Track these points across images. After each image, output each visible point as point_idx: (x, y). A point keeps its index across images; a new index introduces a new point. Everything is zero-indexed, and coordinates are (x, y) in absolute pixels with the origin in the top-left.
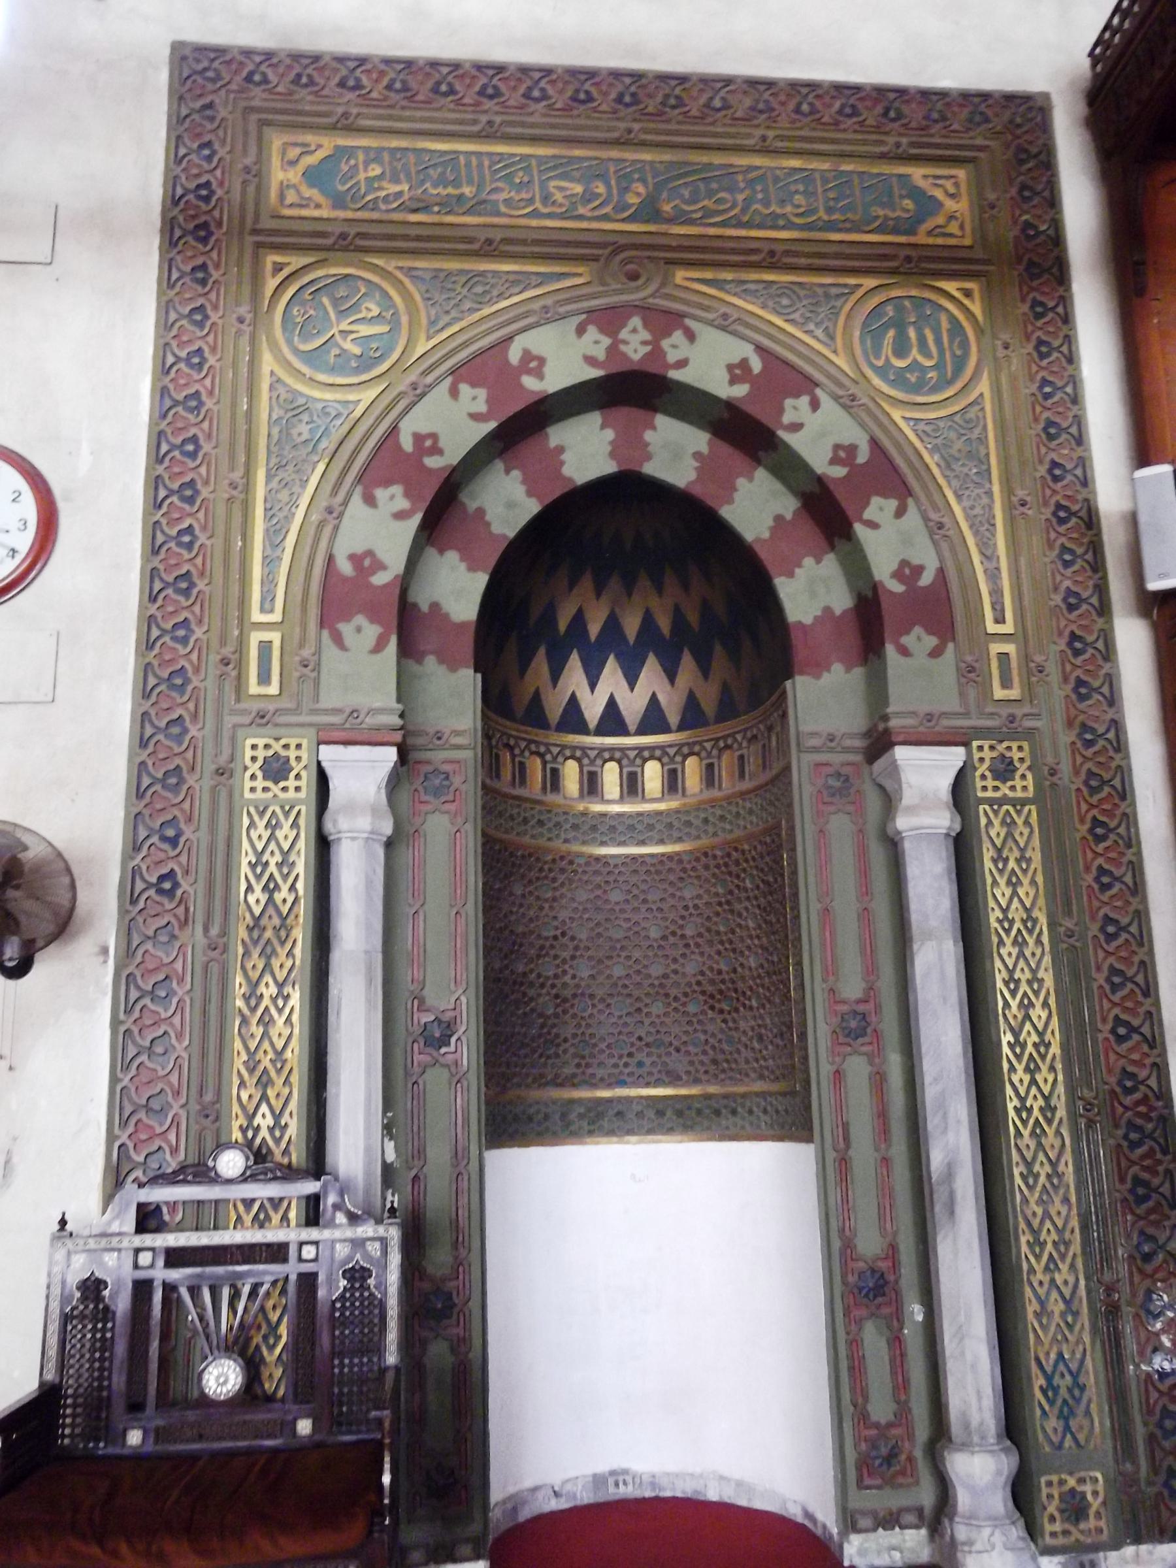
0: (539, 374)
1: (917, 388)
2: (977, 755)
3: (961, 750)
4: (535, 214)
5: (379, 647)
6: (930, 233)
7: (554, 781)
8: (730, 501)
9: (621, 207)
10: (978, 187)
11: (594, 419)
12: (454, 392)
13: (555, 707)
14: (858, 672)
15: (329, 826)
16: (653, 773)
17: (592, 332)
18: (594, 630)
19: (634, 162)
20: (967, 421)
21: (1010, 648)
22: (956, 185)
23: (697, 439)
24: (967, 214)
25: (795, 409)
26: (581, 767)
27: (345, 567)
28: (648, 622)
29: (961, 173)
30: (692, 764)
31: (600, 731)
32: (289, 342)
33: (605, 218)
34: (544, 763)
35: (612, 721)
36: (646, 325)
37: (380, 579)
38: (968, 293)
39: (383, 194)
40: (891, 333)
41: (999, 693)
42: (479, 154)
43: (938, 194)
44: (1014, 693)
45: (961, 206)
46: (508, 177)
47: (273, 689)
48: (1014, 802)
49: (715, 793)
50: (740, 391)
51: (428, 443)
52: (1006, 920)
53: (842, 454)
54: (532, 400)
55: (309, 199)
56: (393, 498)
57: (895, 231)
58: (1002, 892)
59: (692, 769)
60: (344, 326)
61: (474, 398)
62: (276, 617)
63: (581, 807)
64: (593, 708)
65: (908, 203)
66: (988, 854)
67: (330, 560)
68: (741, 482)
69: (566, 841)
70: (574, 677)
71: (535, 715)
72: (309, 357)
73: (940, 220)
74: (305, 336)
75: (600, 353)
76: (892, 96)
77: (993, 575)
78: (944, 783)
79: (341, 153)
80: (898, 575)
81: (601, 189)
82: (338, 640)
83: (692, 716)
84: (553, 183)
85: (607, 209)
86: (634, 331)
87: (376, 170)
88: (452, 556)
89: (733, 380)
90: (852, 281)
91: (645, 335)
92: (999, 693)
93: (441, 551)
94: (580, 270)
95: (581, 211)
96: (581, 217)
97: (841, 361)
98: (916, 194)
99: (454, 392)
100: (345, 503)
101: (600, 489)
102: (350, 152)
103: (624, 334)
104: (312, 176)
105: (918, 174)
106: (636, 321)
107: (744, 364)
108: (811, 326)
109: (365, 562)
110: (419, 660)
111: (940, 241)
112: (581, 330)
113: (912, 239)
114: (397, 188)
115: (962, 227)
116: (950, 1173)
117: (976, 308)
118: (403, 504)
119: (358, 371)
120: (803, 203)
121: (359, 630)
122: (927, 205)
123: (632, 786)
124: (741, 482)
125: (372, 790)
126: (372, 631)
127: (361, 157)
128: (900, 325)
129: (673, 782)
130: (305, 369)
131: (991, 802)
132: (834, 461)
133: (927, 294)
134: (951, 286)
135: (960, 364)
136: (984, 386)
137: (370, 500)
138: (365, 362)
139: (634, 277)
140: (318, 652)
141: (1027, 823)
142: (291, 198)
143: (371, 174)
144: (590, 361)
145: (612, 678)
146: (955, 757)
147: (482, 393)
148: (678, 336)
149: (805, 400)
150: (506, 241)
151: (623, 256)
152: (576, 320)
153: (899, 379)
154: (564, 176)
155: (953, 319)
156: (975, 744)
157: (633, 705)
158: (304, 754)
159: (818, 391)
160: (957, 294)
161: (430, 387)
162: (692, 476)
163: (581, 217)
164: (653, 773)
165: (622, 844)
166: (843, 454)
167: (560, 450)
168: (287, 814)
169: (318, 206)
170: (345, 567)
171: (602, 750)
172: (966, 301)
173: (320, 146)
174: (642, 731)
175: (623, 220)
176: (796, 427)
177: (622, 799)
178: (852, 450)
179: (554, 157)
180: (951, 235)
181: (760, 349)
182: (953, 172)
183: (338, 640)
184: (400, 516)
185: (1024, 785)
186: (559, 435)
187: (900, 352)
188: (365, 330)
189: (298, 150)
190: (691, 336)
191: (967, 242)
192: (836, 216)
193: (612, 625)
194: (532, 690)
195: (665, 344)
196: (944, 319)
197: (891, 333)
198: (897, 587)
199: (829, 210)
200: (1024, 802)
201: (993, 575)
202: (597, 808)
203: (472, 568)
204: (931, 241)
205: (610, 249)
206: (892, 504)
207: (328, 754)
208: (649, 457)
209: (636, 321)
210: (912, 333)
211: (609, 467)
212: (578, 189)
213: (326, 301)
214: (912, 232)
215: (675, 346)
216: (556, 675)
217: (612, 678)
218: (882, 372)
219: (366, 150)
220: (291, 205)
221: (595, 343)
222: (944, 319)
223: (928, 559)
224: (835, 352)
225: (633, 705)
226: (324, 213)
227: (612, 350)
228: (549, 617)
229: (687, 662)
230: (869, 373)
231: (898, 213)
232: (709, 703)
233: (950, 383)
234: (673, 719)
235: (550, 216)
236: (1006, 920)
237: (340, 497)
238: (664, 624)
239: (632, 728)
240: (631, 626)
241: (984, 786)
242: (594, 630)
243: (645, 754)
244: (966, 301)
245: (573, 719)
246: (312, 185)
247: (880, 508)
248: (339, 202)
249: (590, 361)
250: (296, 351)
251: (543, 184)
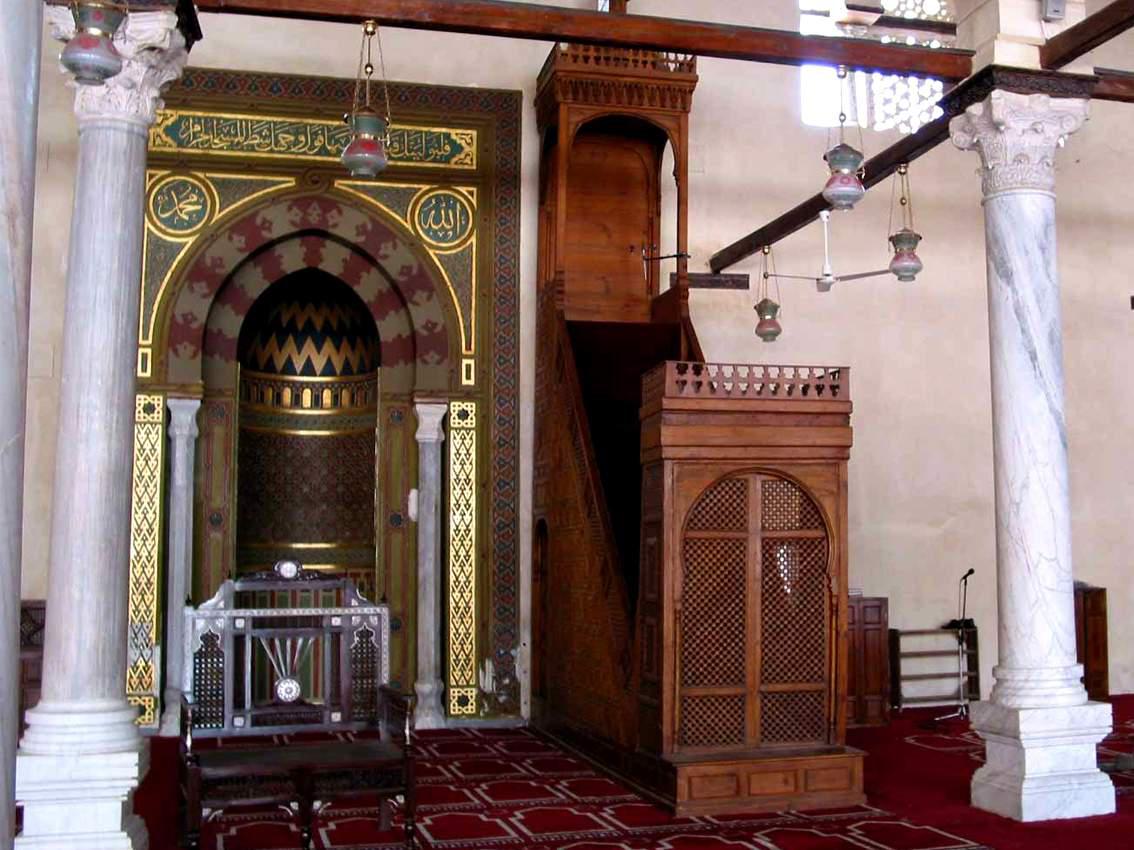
0: (269, 229)
1: (444, 239)
2: (452, 409)
3: (446, 406)
4: (272, 151)
5: (195, 355)
6: (456, 163)
7: (278, 398)
8: (358, 283)
9: (312, 147)
10: (481, 140)
11: (297, 241)
12: (230, 238)
13: (280, 363)
14: (410, 366)
15: (171, 433)
16: (327, 396)
17: (295, 210)
18: (300, 326)
19: (319, 125)
20: (464, 257)
21: (471, 362)
22: (471, 138)
23: (345, 253)
24: (475, 152)
25: (386, 249)
26: (292, 391)
27: (180, 320)
28: (327, 322)
29: (474, 133)
30: (345, 393)
31: (303, 374)
32: (156, 214)
33: (304, 153)
34: (274, 390)
35: (309, 370)
36: (321, 207)
37: (195, 325)
38: (471, 193)
39: (200, 140)
40: (433, 212)
41: (465, 382)
42: (246, 121)
43: (463, 143)
44: (471, 382)
45: (474, 149)
46: (260, 133)
47: (148, 374)
48: (466, 429)
49: (354, 409)
50: (361, 239)
51: (218, 262)
52: (458, 480)
53: (405, 270)
54: (265, 242)
55: (166, 142)
56: (201, 287)
57: (440, 162)
58: (458, 467)
59: (345, 395)
60: (181, 206)
61: (240, 241)
62: (150, 342)
63: (291, 411)
64: (299, 364)
65: (448, 148)
66: (453, 451)
67: (173, 316)
68: (364, 274)
69: (283, 428)
70: (290, 346)
71: (270, 367)
72: (163, 221)
73: (462, 156)
74: (162, 212)
75: (297, 219)
76: (445, 92)
77: (468, 329)
78: (439, 419)
79: (181, 118)
80: (425, 327)
81: (302, 138)
82: (175, 351)
83: (347, 369)
84: (280, 135)
85: (305, 149)
86: (315, 209)
87: (198, 128)
88: (228, 307)
89: (358, 234)
90: (416, 186)
91: (319, 212)
92: (465, 382)
93: (224, 304)
94: (287, 179)
95: (293, 150)
96: (293, 153)
97: (408, 226)
98: (453, 143)
99: (230, 238)
100: (180, 289)
101: (298, 274)
102: (187, 118)
103: (310, 211)
104: (169, 131)
105: (454, 133)
106: (315, 204)
107: (364, 226)
108: (396, 208)
109: (189, 318)
110: (212, 356)
111: (460, 167)
112: (290, 208)
113: (448, 166)
114: (207, 137)
115: (472, 160)
116: (425, 579)
117: (474, 202)
118: (206, 291)
119: (190, 226)
120: (398, 146)
121: (185, 348)
122: (457, 148)
123: (317, 402)
124: (364, 274)
125: (190, 418)
126: (191, 349)
127: (191, 121)
128: (437, 208)
129: (336, 398)
130: (163, 227)
131: (456, 429)
132: (401, 273)
133: (450, 193)
134: (463, 190)
135: (464, 228)
136: (473, 240)
137: (192, 289)
138: (190, 224)
139: (316, 182)
140: (167, 357)
141: (471, 438)
142: (158, 141)
143: (195, 130)
144: (293, 223)
145: (309, 347)
146: (442, 409)
147: (243, 239)
148: (334, 212)
149: (390, 244)
150: (257, 165)
151: (310, 174)
152: (289, 203)
153: (435, 237)
154: (287, 132)
155: (462, 205)
156: (452, 404)
157: (319, 363)
158: (161, 403)
159: (397, 241)
160: (466, 194)
161: (218, 237)
162: (342, 271)
163: (293, 153)
164: (327, 396)
165: (310, 429)
166: (406, 270)
167: (280, 256)
168: (153, 428)
169: (170, 146)
170: (180, 320)
171: (302, 383)
172: (470, 197)
173: (172, 116)
174: (323, 374)
175: (316, 154)
176: (385, 257)
177: (311, 408)
178: (410, 268)
179: (281, 123)
180: (467, 164)
181: (373, 220)
182: (469, 132)
183: (175, 351)
184: (205, 296)
185: (471, 422)
186: (279, 249)
187: (437, 221)
188: (191, 208)
189: (162, 118)
190: (340, 212)
191: (474, 167)
192: (413, 154)
193: (309, 324)
194: (268, 355)
195: (328, 215)
196: (458, 205)
197: (433, 212)
198: (425, 333)
199: (409, 152)
200: (470, 429)
201: (468, 329)
202: (300, 412)
203: (237, 314)
204: (456, 167)
205: (306, 169)
206: (425, 295)
207: (171, 403)
208: (321, 260)
209: (315, 204)
210: (443, 212)
211: (302, 265)
212: (292, 138)
213: (173, 193)
214: (447, 161)
215: (333, 217)
216: (281, 345)
217: (309, 347)
218: (427, 232)
219: (194, 117)
220: (159, 145)
221: (296, 215)
222: (458, 205)
223: (440, 320)
224: (406, 221)
225: (319, 363)
226: (174, 149)
227: (304, 219)
228: (278, 316)
229: (345, 344)
230: (421, 232)
231: (442, 152)
232: (355, 366)
233: (458, 238)
234: (338, 369)
235: (280, 152)
236: (458, 480)
237: (177, 288)
238: (335, 324)
239: (318, 373)
240: (319, 323)
241: (455, 422)
242: (300, 326)
243: (323, 386)
244: (470, 197)
245: (289, 368)
246: (167, 135)
247: (420, 296)
248: (180, 144)
249: (293, 223)
250: (158, 217)
251: (276, 136)
